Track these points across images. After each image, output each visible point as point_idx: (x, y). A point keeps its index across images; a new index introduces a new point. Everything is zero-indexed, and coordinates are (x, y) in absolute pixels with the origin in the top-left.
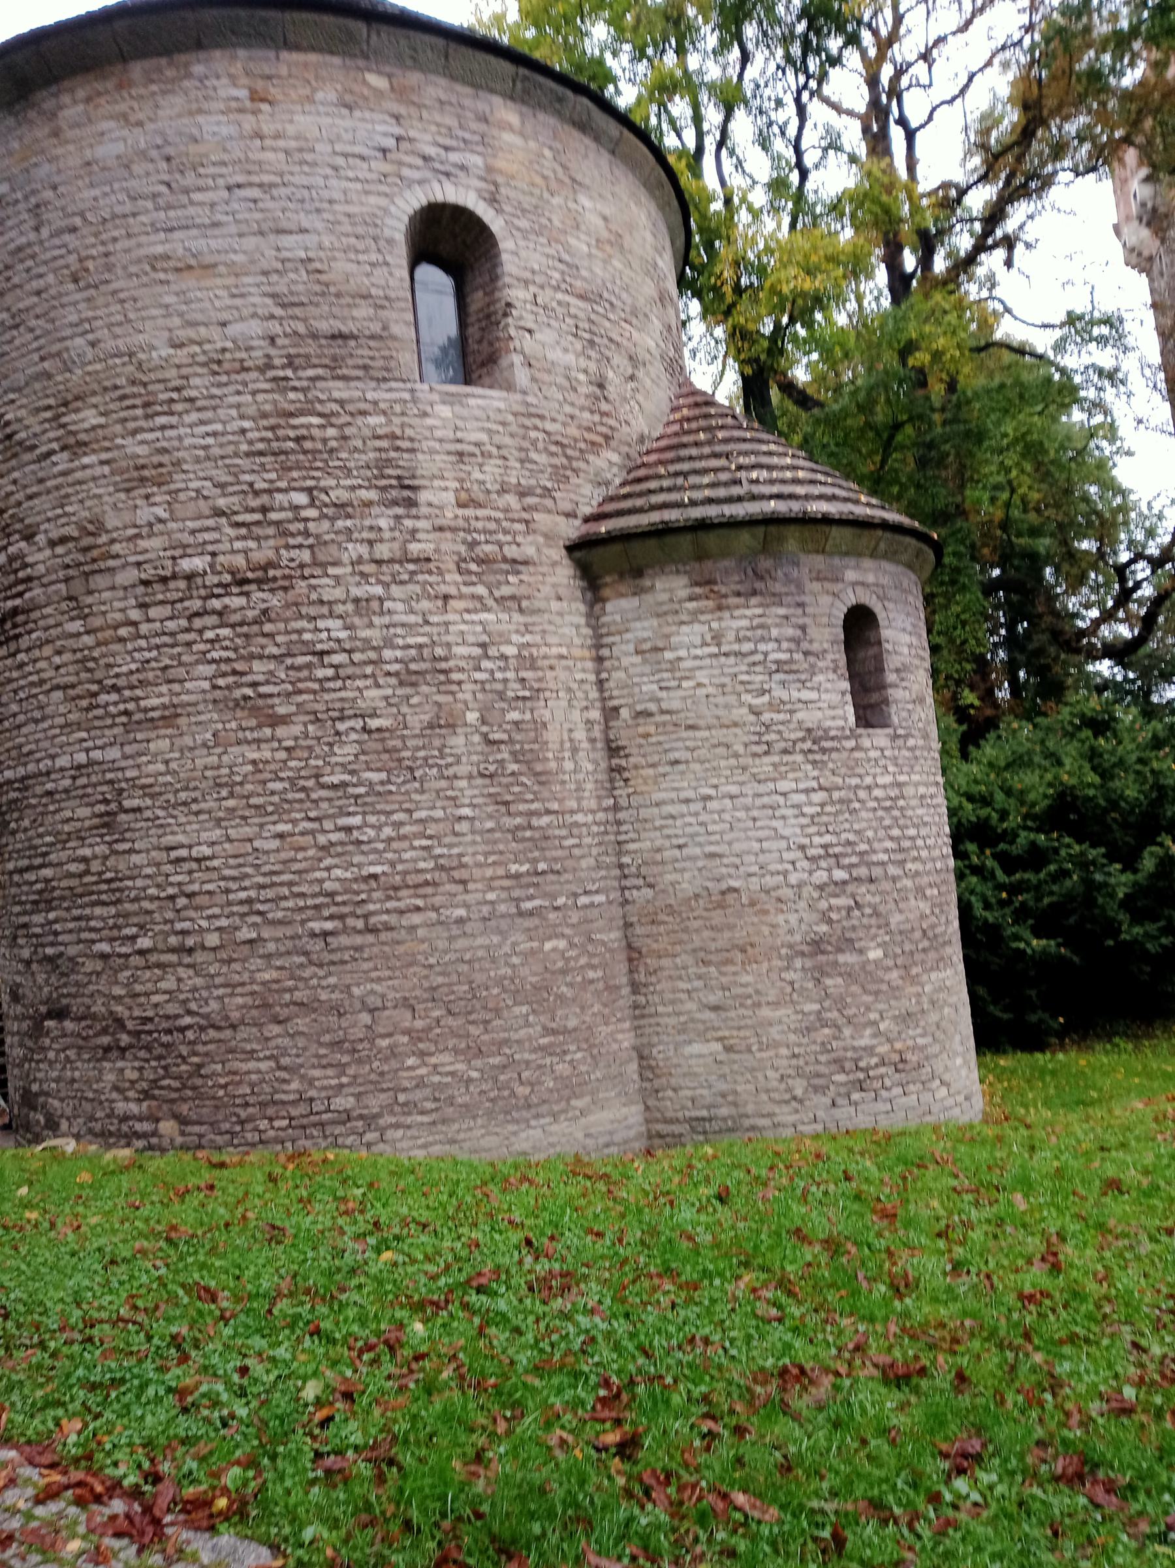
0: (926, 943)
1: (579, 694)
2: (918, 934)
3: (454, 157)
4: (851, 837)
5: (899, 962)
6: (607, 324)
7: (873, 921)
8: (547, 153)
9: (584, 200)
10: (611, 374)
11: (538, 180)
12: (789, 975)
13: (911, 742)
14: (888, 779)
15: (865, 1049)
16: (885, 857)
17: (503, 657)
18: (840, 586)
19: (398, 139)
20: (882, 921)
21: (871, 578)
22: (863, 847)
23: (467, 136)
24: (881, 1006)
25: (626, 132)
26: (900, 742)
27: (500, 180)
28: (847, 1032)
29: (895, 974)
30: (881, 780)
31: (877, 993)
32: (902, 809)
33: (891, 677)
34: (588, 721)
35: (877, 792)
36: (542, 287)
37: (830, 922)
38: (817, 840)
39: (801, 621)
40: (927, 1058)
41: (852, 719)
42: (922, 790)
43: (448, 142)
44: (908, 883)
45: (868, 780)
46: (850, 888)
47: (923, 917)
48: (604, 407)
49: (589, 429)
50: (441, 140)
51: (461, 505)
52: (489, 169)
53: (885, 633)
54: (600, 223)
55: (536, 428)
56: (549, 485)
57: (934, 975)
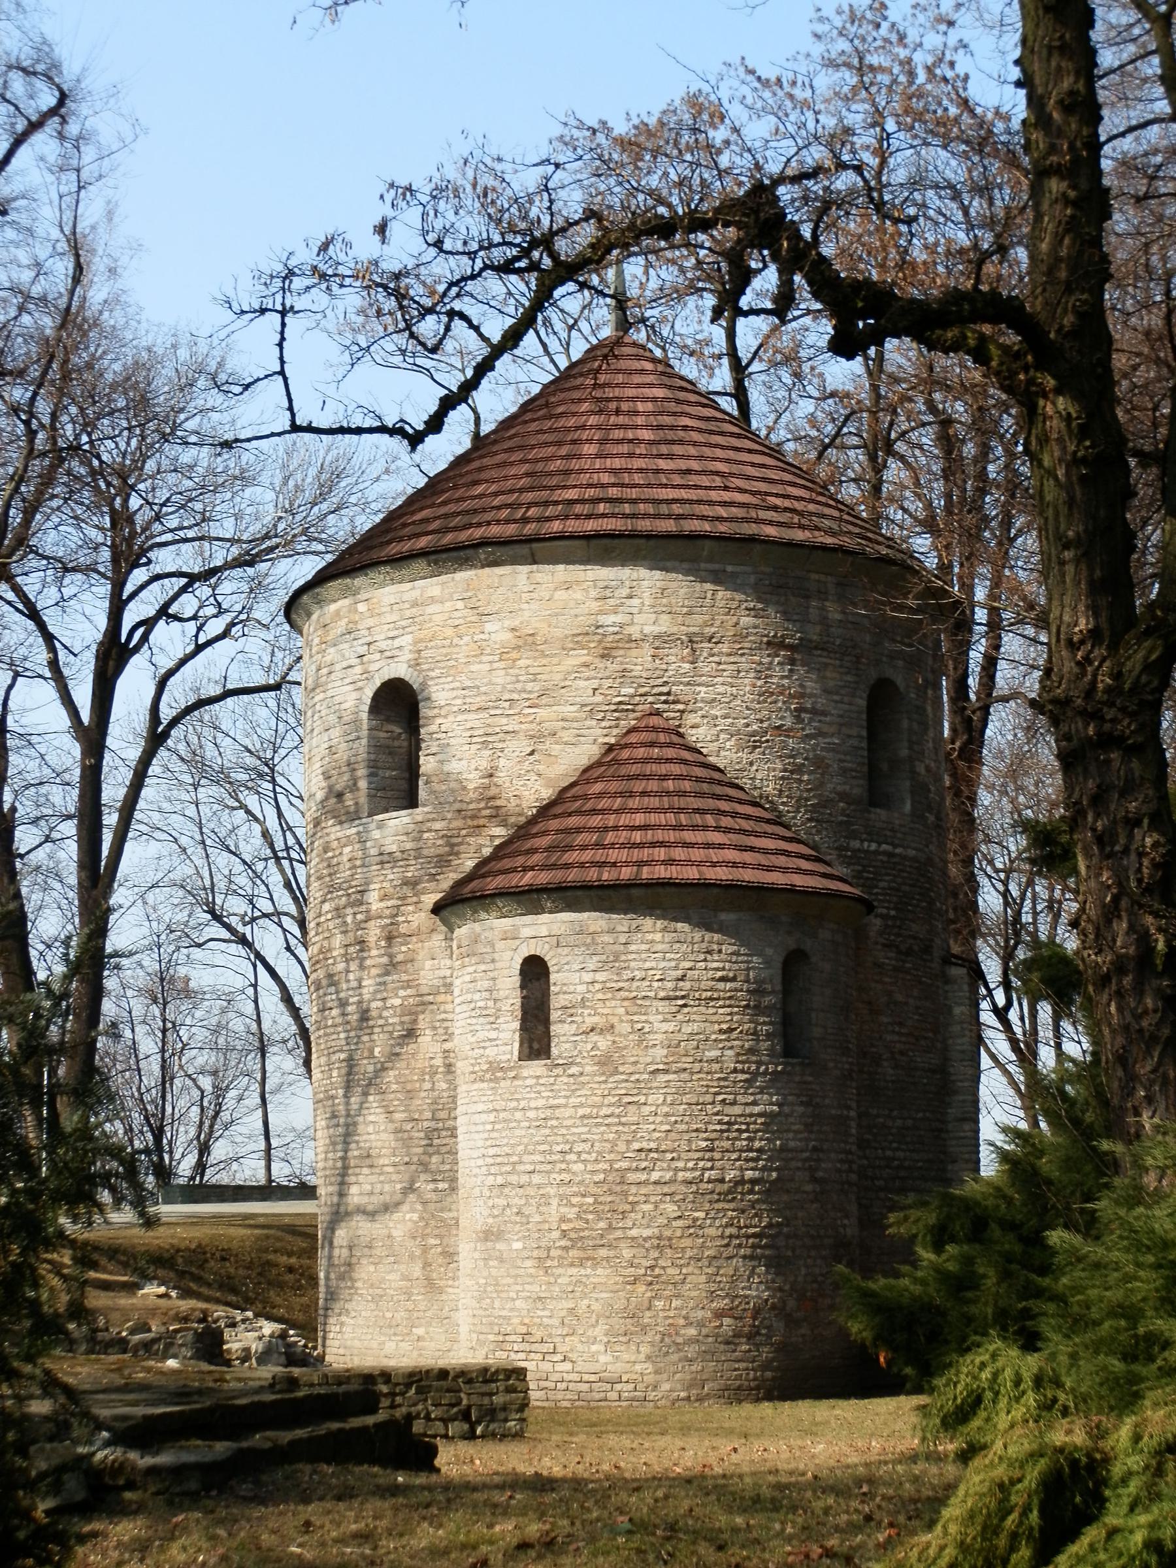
0: (563, 1243)
1: (441, 1031)
2: (556, 1234)
3: (397, 643)
4: (507, 1150)
5: (535, 1253)
6: (504, 721)
7: (518, 1219)
8: (460, 605)
9: (488, 627)
10: (502, 762)
11: (449, 632)
12: (477, 1255)
13: (574, 1070)
14: (541, 1103)
15: (504, 1318)
16: (530, 1168)
17: (393, 1007)
18: (517, 942)
19: (369, 644)
20: (524, 1220)
21: (544, 931)
22: (515, 1159)
23: (404, 623)
24: (519, 1288)
25: (535, 545)
26: (559, 1071)
27: (421, 646)
28: (497, 1304)
29: (528, 1263)
30: (533, 1104)
31: (517, 1276)
32: (552, 1127)
33: (554, 1015)
34: (445, 1051)
35: (531, 1114)
36: (445, 717)
37: (495, 1217)
38: (492, 1151)
39: (491, 974)
40: (550, 1336)
41: (516, 1053)
42: (581, 1112)
43: (396, 633)
44: (552, 1191)
45: (523, 1104)
46: (506, 1190)
47: (563, 1220)
48: (493, 791)
49: (473, 817)
50: (391, 634)
51: (381, 900)
52: (415, 643)
53: (553, 977)
54: (509, 635)
55: (430, 831)
56: (433, 871)
57: (573, 1271)
